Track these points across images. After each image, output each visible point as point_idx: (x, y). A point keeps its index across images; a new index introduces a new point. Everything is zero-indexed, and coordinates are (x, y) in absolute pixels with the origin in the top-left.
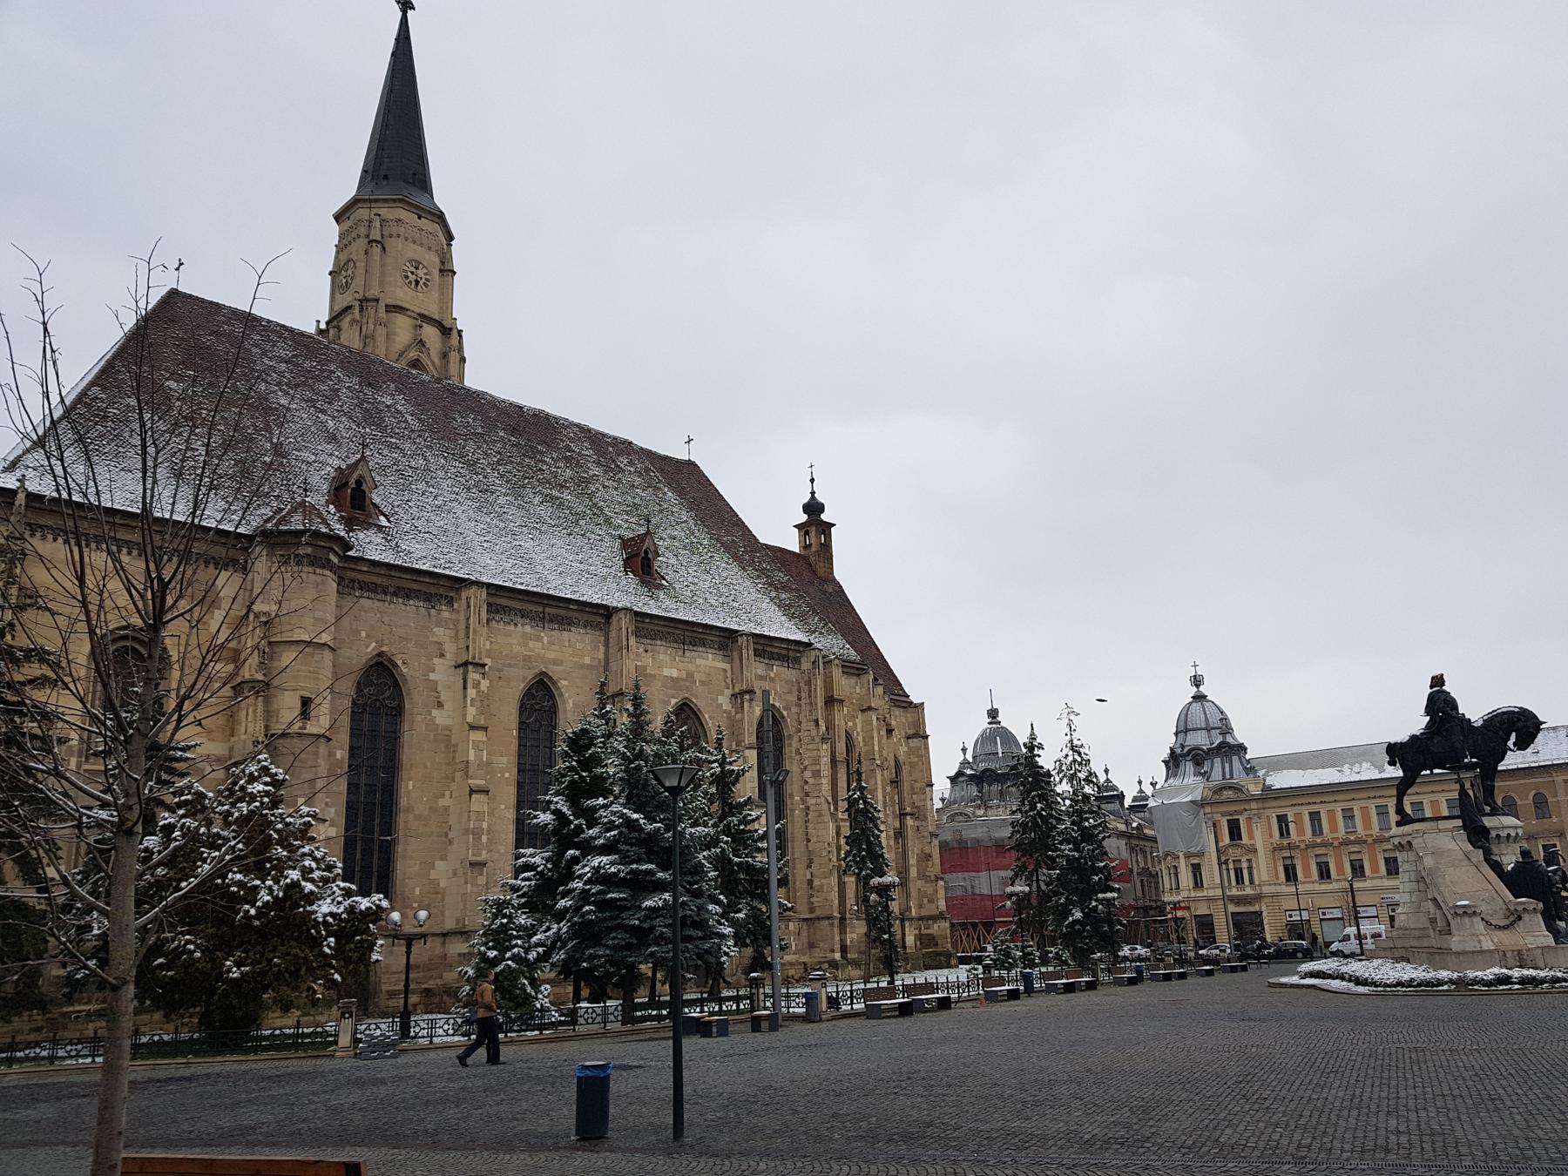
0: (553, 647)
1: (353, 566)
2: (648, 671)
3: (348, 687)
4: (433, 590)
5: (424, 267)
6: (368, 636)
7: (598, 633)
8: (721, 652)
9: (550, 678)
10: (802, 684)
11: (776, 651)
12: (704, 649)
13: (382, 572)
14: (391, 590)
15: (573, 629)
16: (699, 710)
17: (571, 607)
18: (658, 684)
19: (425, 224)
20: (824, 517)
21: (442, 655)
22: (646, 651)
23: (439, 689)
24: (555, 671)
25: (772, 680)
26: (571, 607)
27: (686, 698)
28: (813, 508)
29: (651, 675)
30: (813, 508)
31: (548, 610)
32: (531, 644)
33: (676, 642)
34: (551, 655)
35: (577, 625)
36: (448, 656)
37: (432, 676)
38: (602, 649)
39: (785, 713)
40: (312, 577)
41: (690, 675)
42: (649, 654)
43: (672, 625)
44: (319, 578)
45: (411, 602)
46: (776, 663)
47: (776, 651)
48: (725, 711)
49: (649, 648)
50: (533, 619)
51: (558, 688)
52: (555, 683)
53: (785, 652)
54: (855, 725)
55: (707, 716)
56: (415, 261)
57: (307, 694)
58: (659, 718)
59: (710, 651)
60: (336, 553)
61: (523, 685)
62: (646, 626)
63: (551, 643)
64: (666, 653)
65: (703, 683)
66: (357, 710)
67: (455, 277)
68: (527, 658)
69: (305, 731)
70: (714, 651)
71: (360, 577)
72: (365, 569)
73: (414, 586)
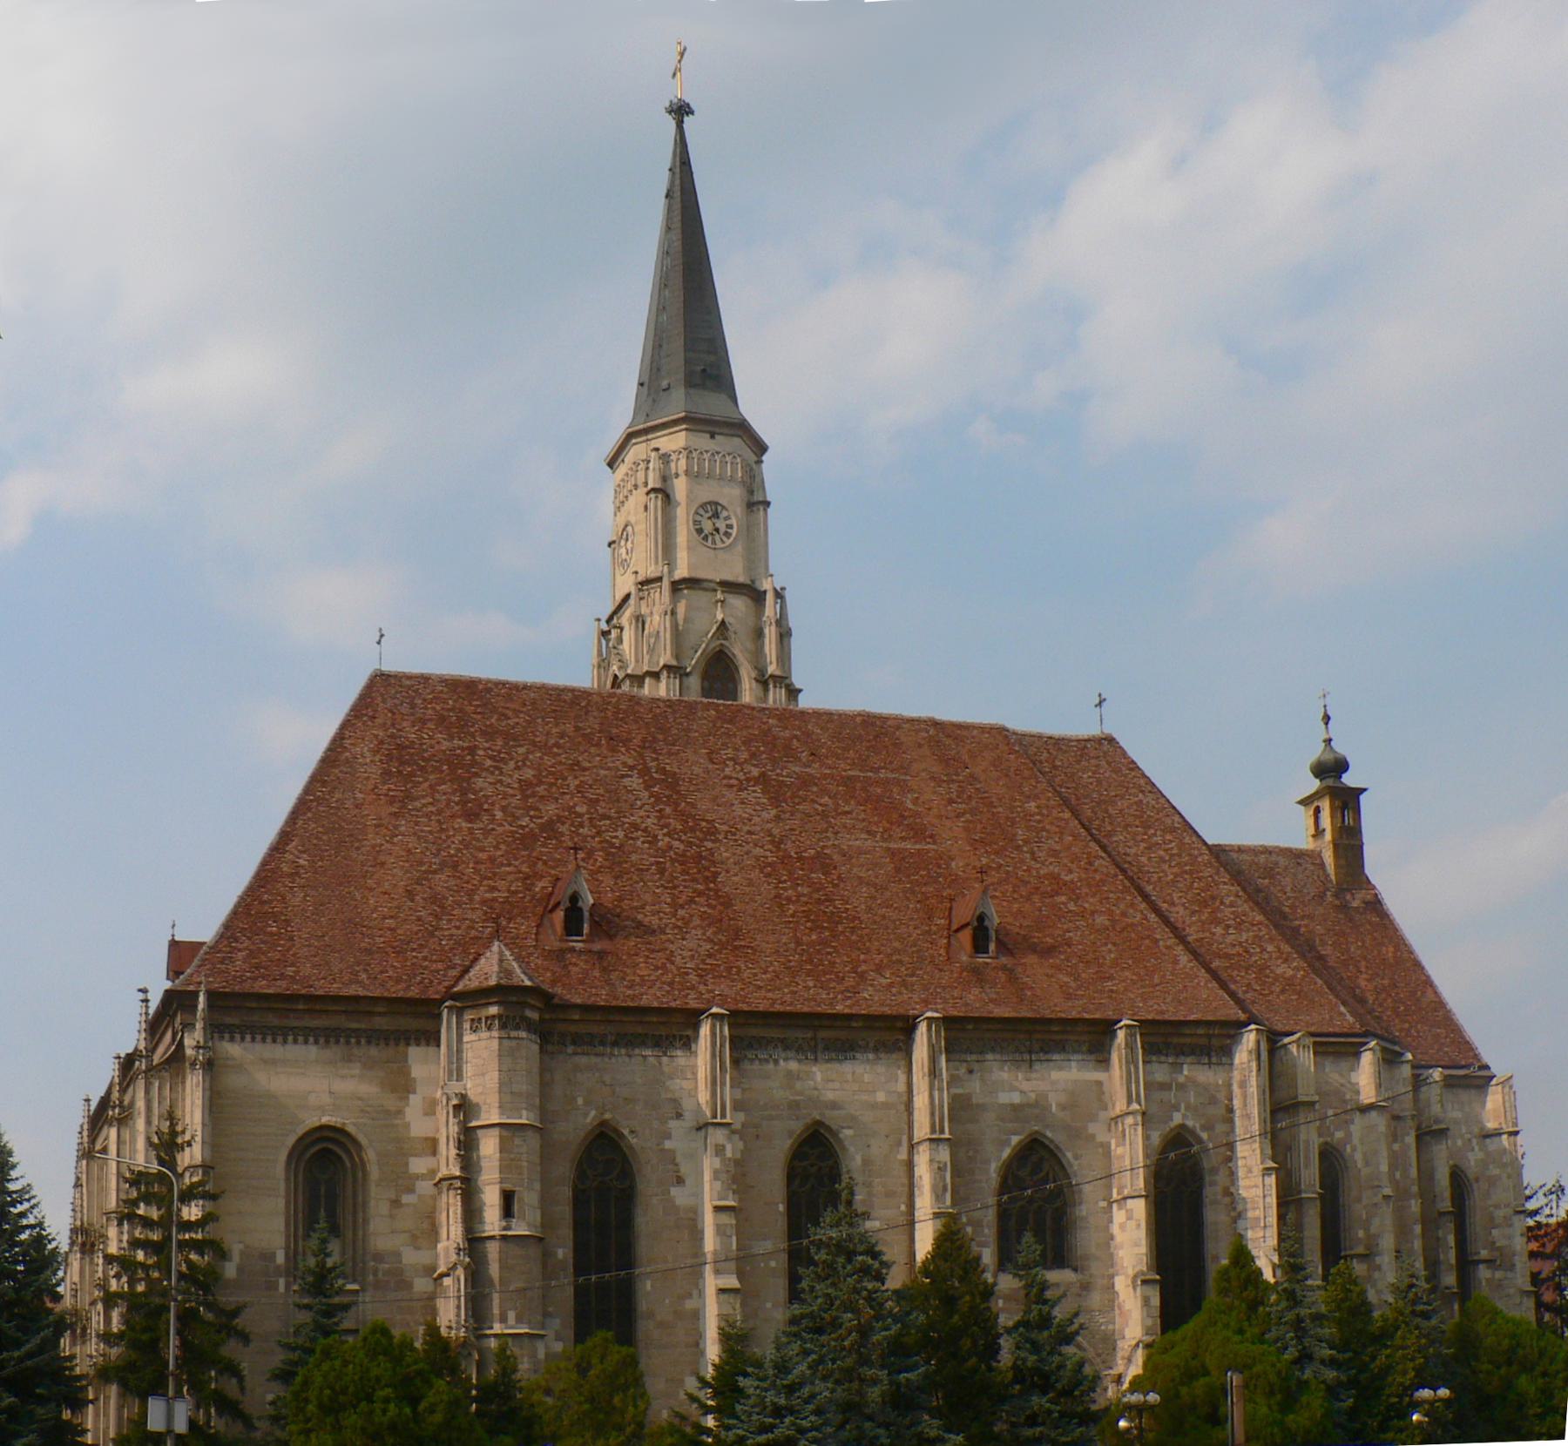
0: (831, 1085)
1: (561, 1016)
2: (974, 1101)
3: (564, 1169)
4: (663, 1031)
6: (587, 1103)
7: (894, 1056)
8: (1093, 1057)
9: (828, 1128)
10: (1236, 1088)
11: (1188, 1040)
13: (599, 1018)
14: (610, 1038)
15: (858, 1055)
16: (1057, 1147)
17: (854, 1024)
19: (724, 443)
21: (679, 1116)
22: (971, 1072)
23: (678, 1160)
24: (831, 1119)
25: (1181, 1087)
26: (854, 1024)
27: (1037, 1132)
29: (978, 1105)
31: (822, 1034)
33: (1017, 1051)
34: (830, 1096)
35: (865, 1049)
36: (687, 1115)
37: (668, 1145)
38: (902, 1077)
39: (1204, 1136)
40: (506, 1042)
42: (976, 1076)
44: (514, 1043)
45: (637, 1051)
46: (1189, 1059)
47: (1188, 1040)
48: (1102, 1145)
49: (976, 1067)
50: (799, 1050)
51: (840, 1141)
52: (835, 1134)
53: (1204, 1041)
57: (508, 1187)
59: (1076, 1057)
60: (533, 1007)
61: (789, 1142)
64: (1002, 1069)
65: (1063, 1107)
66: (579, 1200)
67: (770, 510)
68: (794, 1106)
69: (510, 1233)
70: (1080, 1057)
71: (573, 1028)
72: (577, 1017)
73: (640, 1030)
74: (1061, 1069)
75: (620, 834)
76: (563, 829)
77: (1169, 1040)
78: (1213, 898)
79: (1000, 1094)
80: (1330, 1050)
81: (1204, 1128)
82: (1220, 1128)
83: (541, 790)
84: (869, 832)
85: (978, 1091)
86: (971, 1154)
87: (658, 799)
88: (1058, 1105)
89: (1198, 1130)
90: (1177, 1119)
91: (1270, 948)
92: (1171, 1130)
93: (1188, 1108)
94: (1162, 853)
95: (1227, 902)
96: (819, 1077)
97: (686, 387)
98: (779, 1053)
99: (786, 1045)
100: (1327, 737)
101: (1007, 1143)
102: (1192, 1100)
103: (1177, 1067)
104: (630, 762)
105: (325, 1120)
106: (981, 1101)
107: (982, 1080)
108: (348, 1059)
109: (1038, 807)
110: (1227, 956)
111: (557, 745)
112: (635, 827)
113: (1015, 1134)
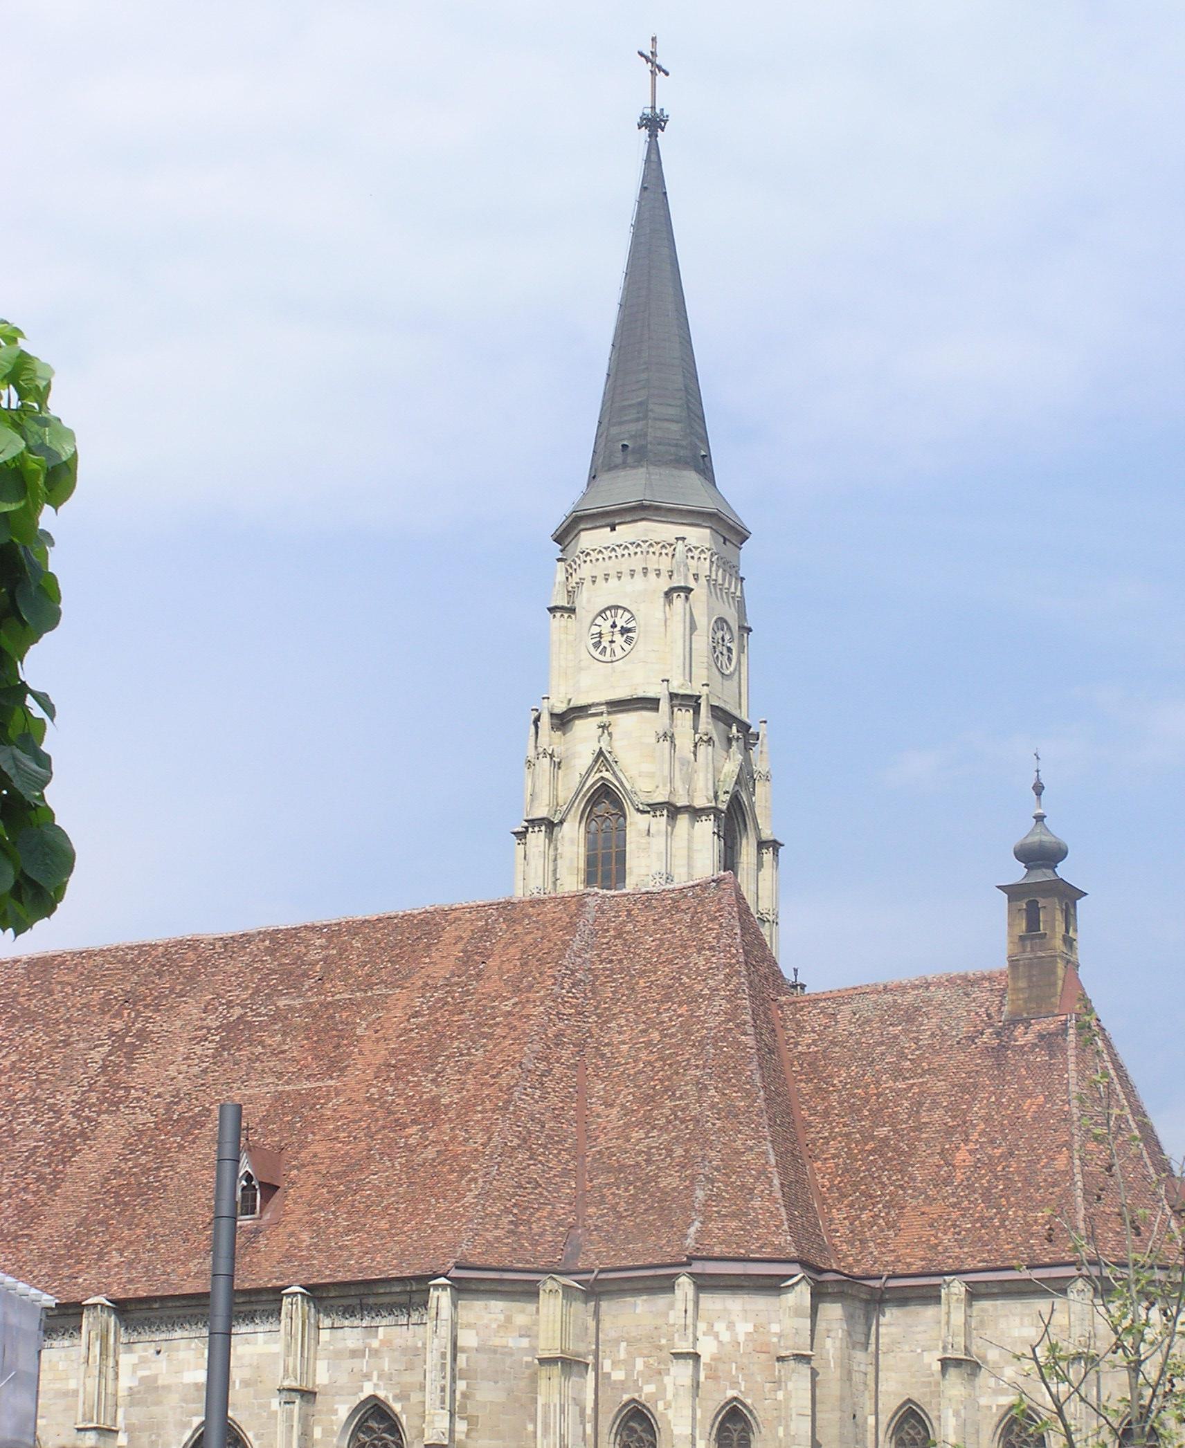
2: (160, 1382)
5: (625, 610)
12: (250, 1328)
15: (55, 1344)
18: (173, 1399)
20: (1064, 870)
22: (158, 1352)
25: (375, 1353)
29: (164, 1387)
39: (397, 1407)
43: (194, 1302)
46: (385, 1322)
49: (164, 1346)
53: (404, 1298)
54: (662, 1389)
55: (250, 1435)
56: (609, 608)
62: (157, 1313)
75: (29, 1120)
77: (364, 1301)
78: (666, 1091)
79: (185, 1374)
80: (640, 1286)
81: (397, 1398)
82: (415, 1397)
84: (280, 1075)
85: (164, 1372)
86: (153, 1437)
87: (104, 1067)
89: (391, 1402)
90: (368, 1390)
91: (679, 1151)
92: (363, 1403)
93: (379, 1377)
94: (656, 1036)
95: (678, 1093)
101: (185, 1425)
102: (386, 1369)
104: (118, 1025)
106: (166, 1383)
107: (169, 1359)
109: (515, 1004)
110: (622, 1168)
111: (67, 1021)
112: (51, 1108)
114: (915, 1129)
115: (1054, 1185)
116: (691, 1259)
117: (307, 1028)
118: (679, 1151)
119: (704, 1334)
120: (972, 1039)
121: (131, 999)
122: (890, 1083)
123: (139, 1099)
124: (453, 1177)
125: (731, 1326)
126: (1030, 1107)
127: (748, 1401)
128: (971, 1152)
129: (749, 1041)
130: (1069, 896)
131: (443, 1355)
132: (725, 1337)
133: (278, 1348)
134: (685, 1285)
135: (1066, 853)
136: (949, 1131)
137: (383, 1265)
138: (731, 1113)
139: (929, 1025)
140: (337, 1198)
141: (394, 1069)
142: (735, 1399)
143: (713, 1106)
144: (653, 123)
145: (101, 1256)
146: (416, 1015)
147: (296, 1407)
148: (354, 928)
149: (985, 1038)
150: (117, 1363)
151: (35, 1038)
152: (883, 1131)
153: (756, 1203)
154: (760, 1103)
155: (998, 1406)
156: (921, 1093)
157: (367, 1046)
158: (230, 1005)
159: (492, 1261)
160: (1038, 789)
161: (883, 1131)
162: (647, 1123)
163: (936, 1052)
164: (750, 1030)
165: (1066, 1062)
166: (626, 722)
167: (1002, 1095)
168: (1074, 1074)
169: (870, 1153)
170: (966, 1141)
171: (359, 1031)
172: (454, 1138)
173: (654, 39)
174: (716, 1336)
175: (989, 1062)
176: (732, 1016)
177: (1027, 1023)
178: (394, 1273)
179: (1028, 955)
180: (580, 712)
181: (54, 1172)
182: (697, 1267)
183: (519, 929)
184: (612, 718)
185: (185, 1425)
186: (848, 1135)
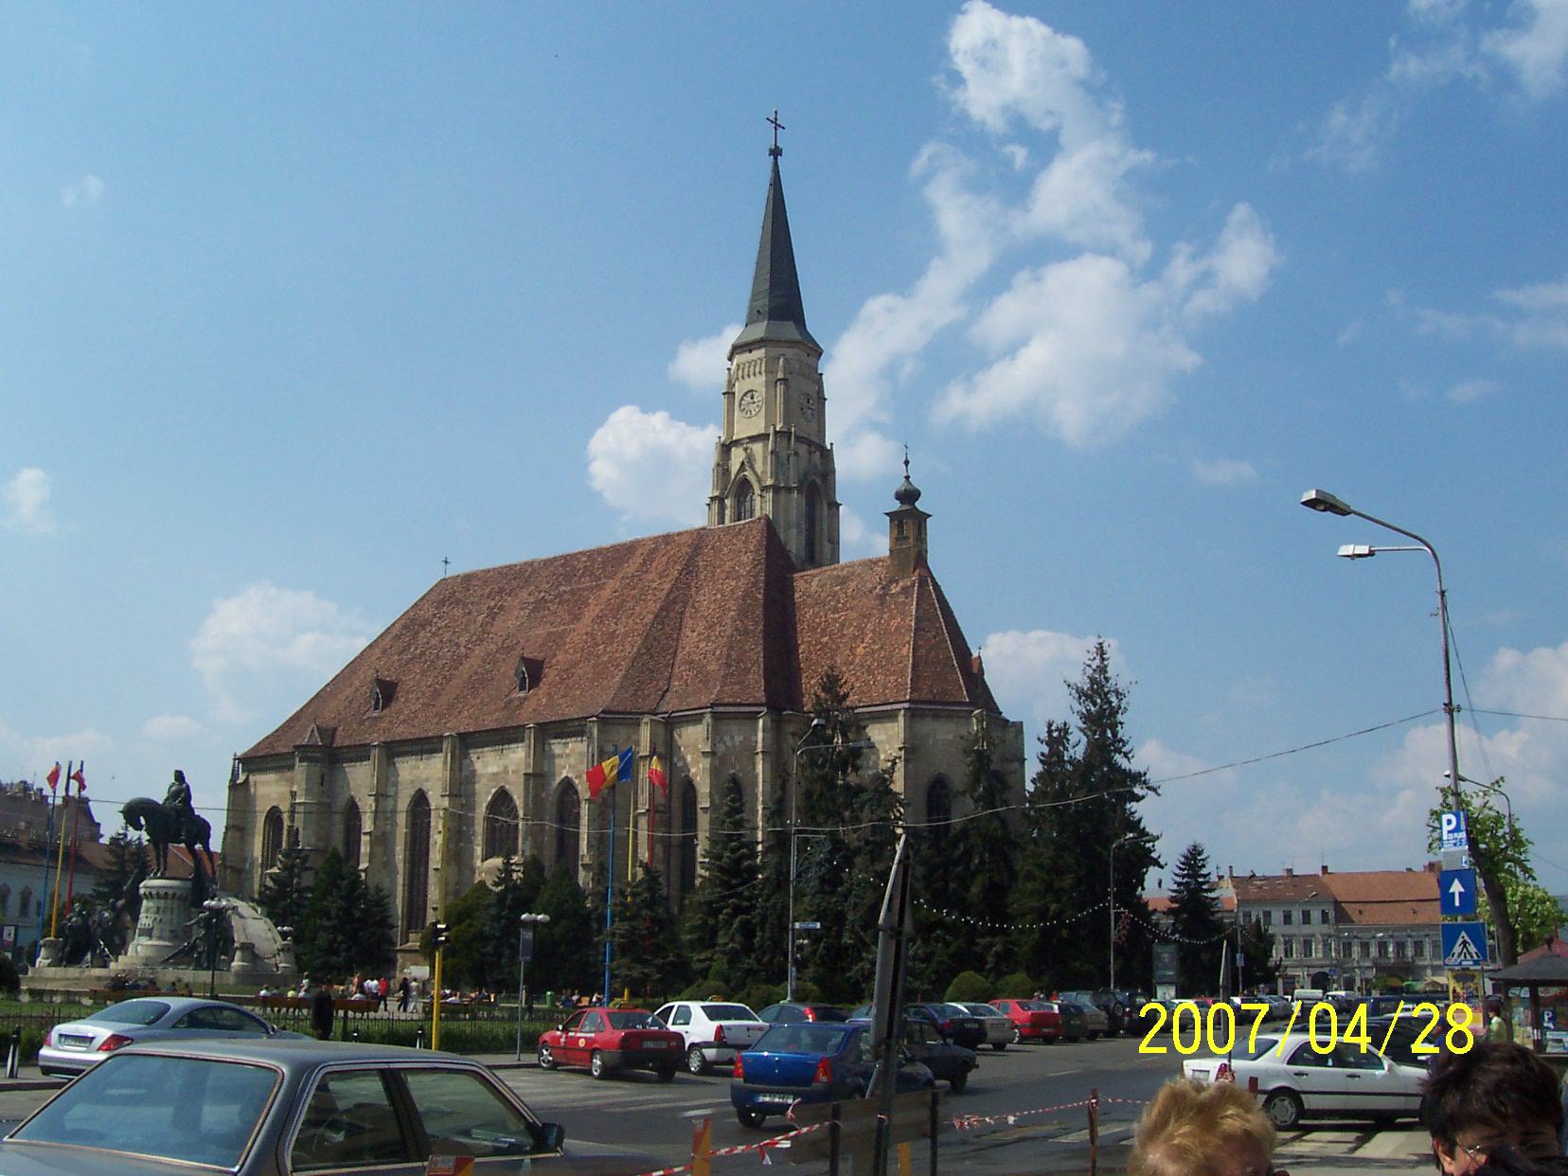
18: (484, 781)
22: (478, 758)
25: (568, 755)
27: (502, 787)
28: (908, 496)
30: (908, 496)
32: (415, 772)
34: (424, 777)
39: (577, 782)
41: (506, 769)
46: (574, 739)
49: (481, 755)
53: (580, 728)
54: (698, 768)
58: (485, 805)
63: (425, 768)
68: (412, 782)
74: (514, 752)
76: (427, 653)
81: (576, 777)
83: (440, 632)
88: (513, 772)
90: (564, 775)
91: (718, 653)
92: (563, 780)
94: (719, 596)
96: (422, 767)
97: (769, 319)
98: (408, 758)
99: (413, 753)
100: (905, 474)
101: (489, 793)
103: (566, 744)
105: (275, 804)
108: (280, 780)
112: (456, 644)
113: (493, 787)
114: (841, 638)
115: (901, 662)
116: (712, 706)
117: (569, 600)
118: (718, 653)
119: (719, 742)
120: (871, 592)
121: (501, 591)
122: (832, 616)
123: (492, 638)
124: (613, 668)
125: (732, 738)
126: (894, 623)
127: (741, 775)
128: (865, 648)
129: (760, 596)
130: (922, 518)
131: (593, 756)
132: (729, 743)
133: (523, 755)
134: (708, 719)
135: (920, 494)
136: (855, 638)
137: (573, 712)
138: (746, 632)
139: (852, 585)
140: (562, 680)
141: (600, 619)
142: (734, 774)
143: (737, 630)
144: (776, 152)
145: (460, 712)
146: (615, 592)
147: (531, 781)
148: (599, 551)
149: (877, 590)
150: (461, 764)
151: (458, 612)
152: (825, 639)
153: (750, 676)
154: (761, 627)
155: (869, 776)
156: (845, 619)
157: (591, 607)
158: (540, 592)
159: (621, 709)
160: (907, 463)
161: (825, 639)
162: (708, 639)
163: (854, 599)
164: (762, 591)
165: (912, 601)
166: (757, 448)
167: (882, 618)
168: (914, 606)
169: (819, 650)
170: (863, 642)
171: (590, 601)
172: (617, 650)
173: (776, 112)
174: (725, 743)
175: (878, 602)
176: (755, 584)
177: (897, 582)
178: (576, 717)
179: (898, 547)
180: (737, 443)
181: (450, 674)
182: (716, 709)
183: (669, 547)
184: (749, 445)
185: (489, 793)
186: (809, 642)
